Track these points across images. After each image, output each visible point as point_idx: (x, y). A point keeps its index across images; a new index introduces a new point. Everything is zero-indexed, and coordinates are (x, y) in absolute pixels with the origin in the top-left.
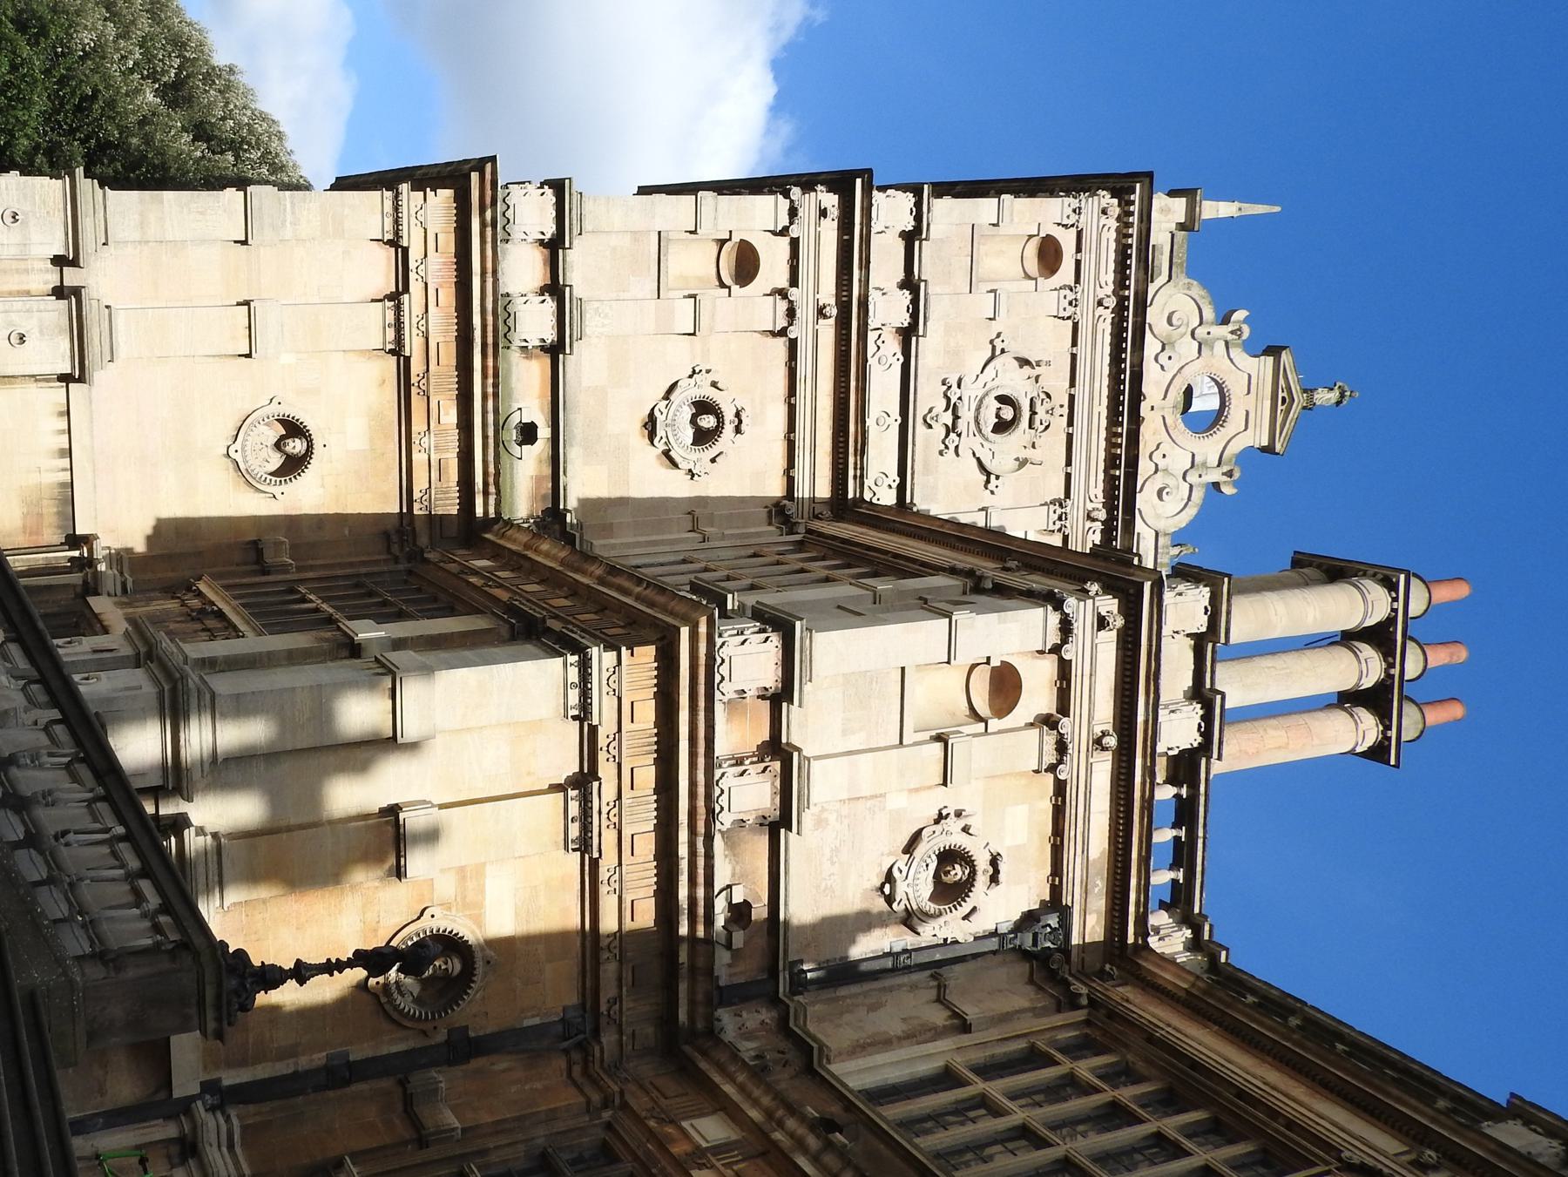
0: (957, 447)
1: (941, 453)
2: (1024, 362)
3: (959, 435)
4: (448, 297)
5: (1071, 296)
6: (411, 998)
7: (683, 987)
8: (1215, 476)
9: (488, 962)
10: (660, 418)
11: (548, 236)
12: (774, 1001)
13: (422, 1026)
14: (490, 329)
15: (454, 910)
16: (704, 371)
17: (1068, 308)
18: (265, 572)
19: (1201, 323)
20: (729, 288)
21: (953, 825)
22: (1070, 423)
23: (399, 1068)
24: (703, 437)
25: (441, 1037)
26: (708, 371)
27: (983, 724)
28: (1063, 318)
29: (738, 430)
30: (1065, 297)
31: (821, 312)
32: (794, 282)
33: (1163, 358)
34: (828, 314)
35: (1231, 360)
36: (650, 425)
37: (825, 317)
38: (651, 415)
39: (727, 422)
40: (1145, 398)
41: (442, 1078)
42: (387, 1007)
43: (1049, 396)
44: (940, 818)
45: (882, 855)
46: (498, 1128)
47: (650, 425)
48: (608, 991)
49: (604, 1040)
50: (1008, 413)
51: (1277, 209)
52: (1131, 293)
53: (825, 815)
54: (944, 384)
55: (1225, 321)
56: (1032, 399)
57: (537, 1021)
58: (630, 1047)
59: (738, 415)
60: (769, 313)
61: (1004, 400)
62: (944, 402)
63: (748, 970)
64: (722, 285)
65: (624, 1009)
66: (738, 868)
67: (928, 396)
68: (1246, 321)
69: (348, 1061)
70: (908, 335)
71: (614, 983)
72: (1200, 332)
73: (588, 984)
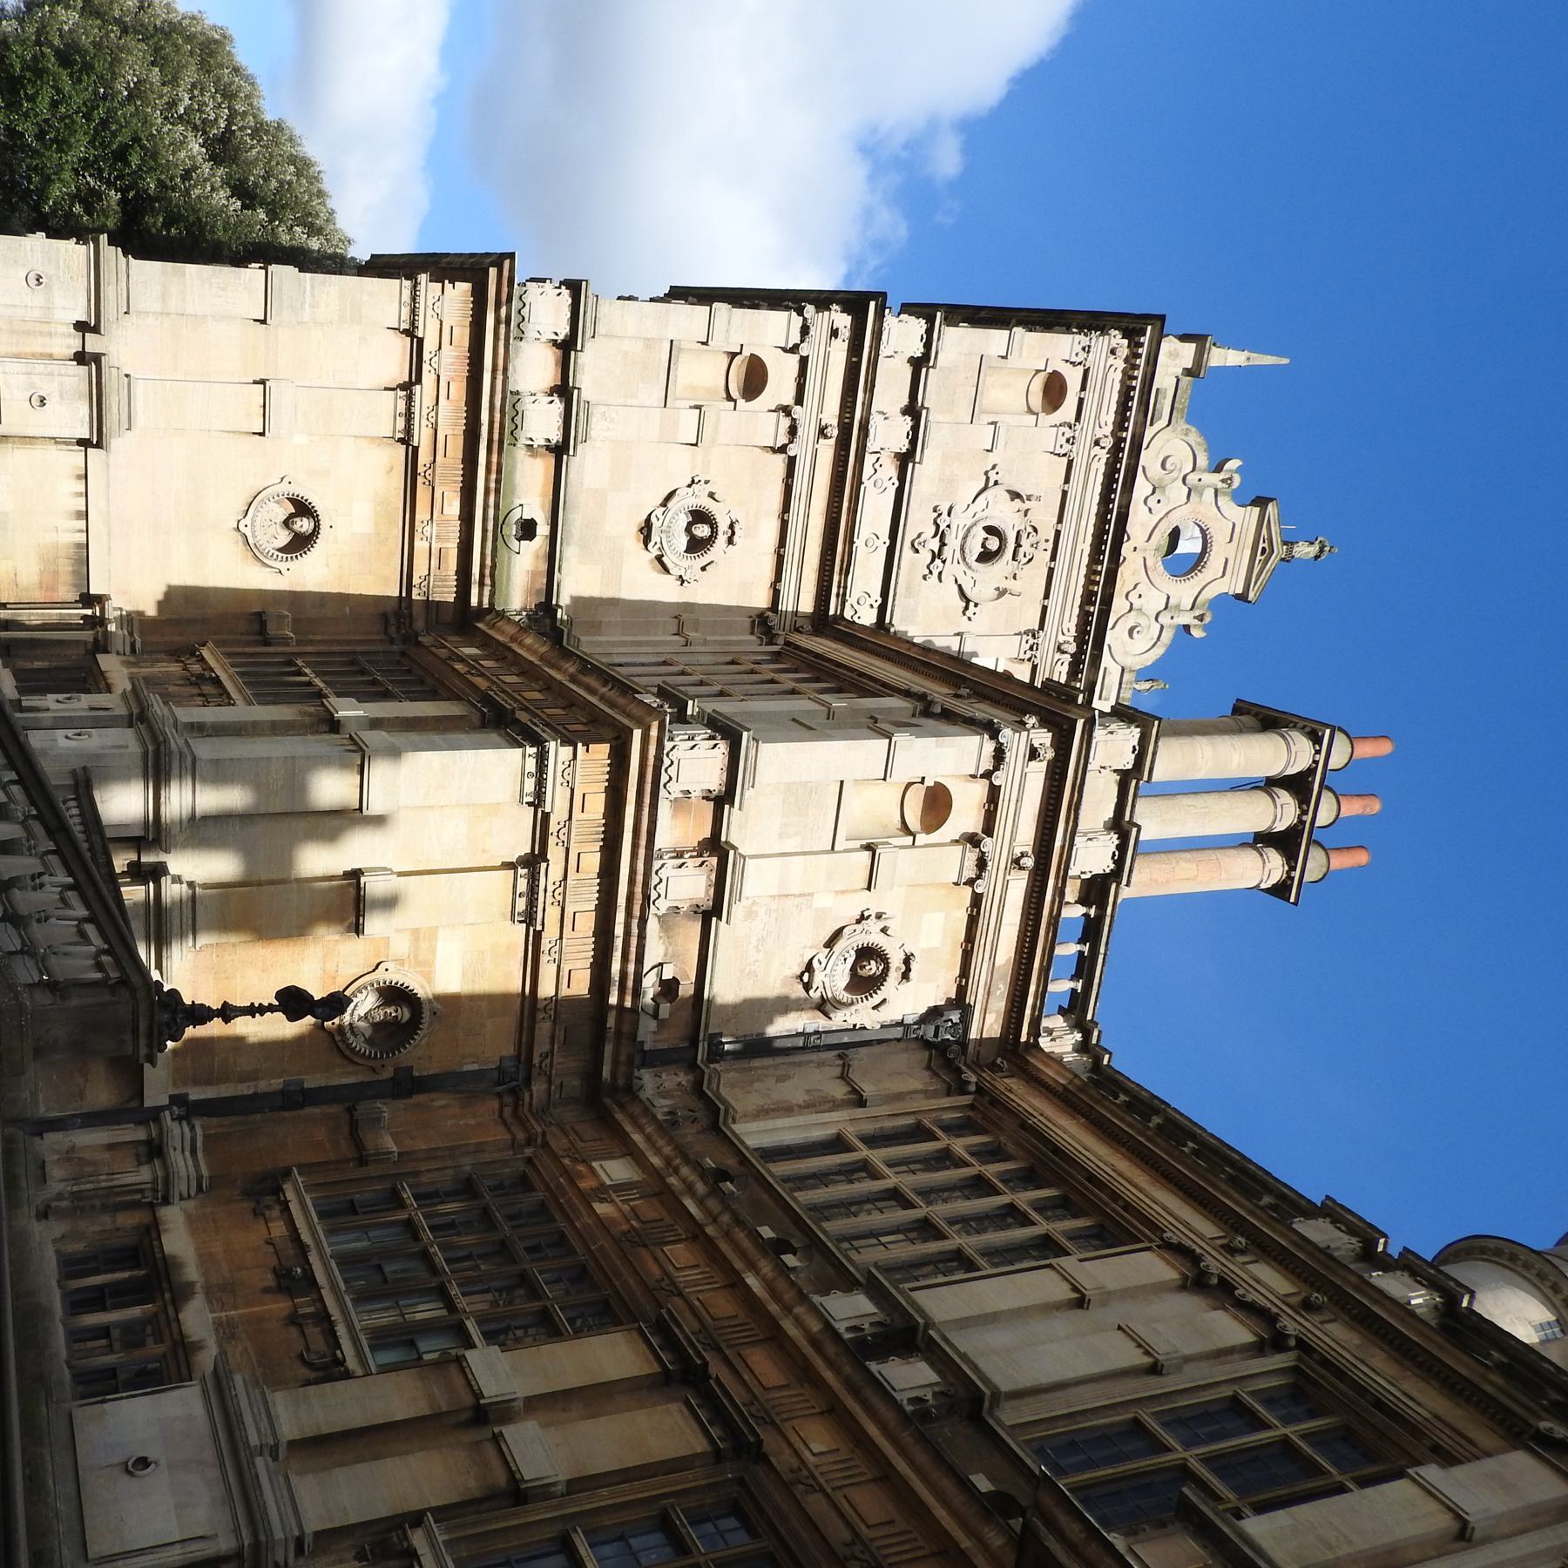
0: (940, 573)
1: (924, 577)
2: (1015, 495)
3: (944, 562)
5: (1069, 433)
6: (363, 1039)
7: (608, 1049)
8: (1187, 619)
10: (656, 524)
12: (692, 1066)
13: (371, 1063)
14: (497, 425)
16: (702, 482)
17: (1065, 445)
18: (267, 643)
19: (1193, 470)
20: (735, 401)
21: (873, 926)
22: (1053, 558)
23: (349, 1097)
24: (696, 546)
25: (388, 1074)
26: (707, 482)
27: (912, 838)
28: (1059, 455)
29: (730, 541)
30: (1063, 434)
31: (822, 432)
32: (799, 400)
33: (1152, 502)
34: (829, 435)
35: (1218, 508)
36: (646, 530)
37: (826, 437)
38: (648, 522)
39: (720, 533)
40: (1129, 539)
41: (386, 1110)
42: (340, 1044)
43: (1035, 530)
44: (862, 918)
45: (805, 947)
46: (431, 1154)
47: (646, 530)
48: (542, 1046)
49: (534, 1088)
50: (993, 544)
51: (1285, 361)
52: (1128, 435)
53: (754, 909)
54: (935, 511)
55: (1218, 469)
56: (1018, 532)
57: (475, 1067)
58: (557, 1096)
59: (731, 526)
60: (771, 429)
61: (991, 530)
62: (933, 529)
63: (672, 1038)
64: (729, 398)
65: (554, 1063)
66: (670, 949)
67: (918, 521)
68: (1239, 470)
69: (303, 1088)
70: (905, 460)
71: (548, 1040)
72: (1192, 478)
73: (524, 1040)
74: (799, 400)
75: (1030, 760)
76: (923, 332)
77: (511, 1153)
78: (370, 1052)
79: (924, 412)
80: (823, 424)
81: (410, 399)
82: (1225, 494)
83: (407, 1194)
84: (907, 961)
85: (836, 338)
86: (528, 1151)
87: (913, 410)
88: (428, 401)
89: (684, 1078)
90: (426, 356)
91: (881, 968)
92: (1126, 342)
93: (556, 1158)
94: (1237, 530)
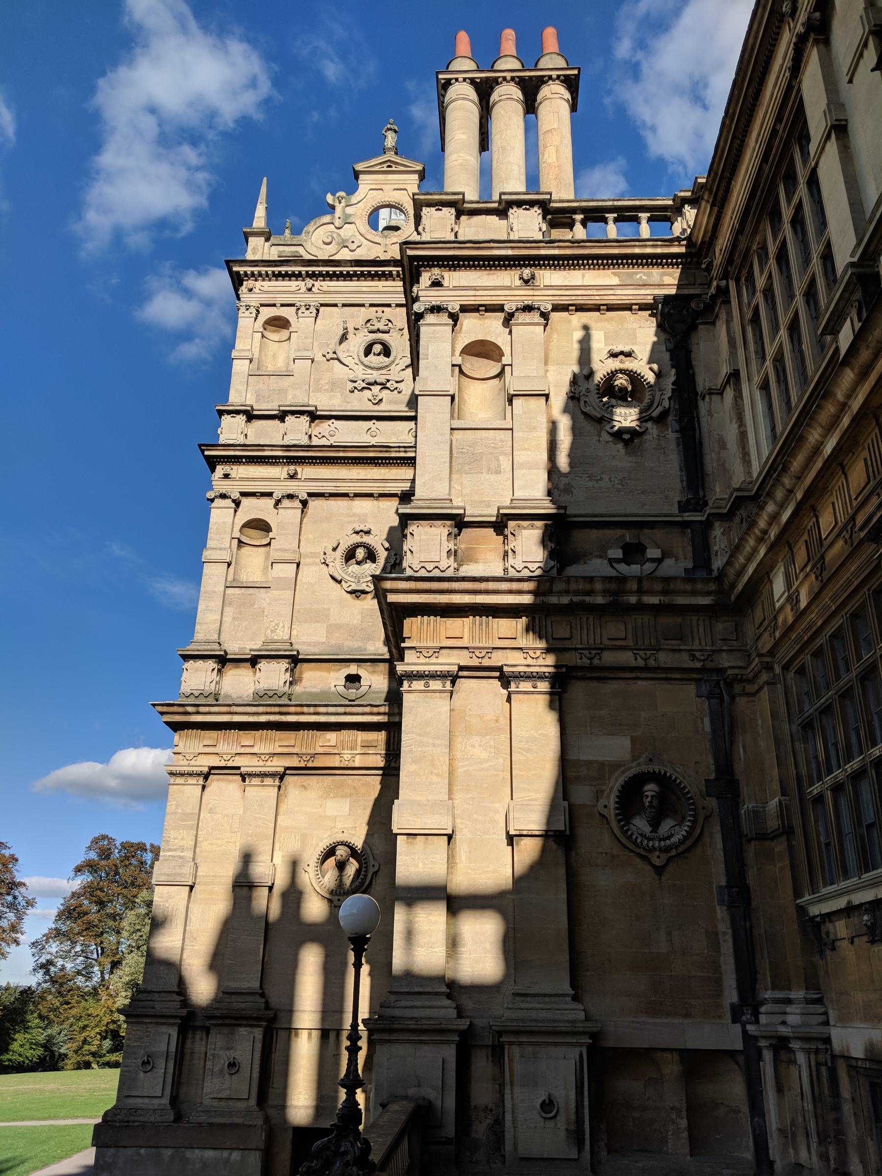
0: (397, 382)
1: (399, 392)
2: (344, 338)
3: (388, 381)
4: (247, 738)
5: (303, 309)
6: (677, 828)
9: (651, 760)
10: (354, 587)
11: (215, 665)
13: (701, 820)
14: (269, 709)
15: (603, 788)
16: (325, 556)
17: (310, 310)
19: (333, 223)
20: (271, 539)
22: (389, 305)
26: (325, 554)
27: (506, 367)
28: (317, 316)
29: (368, 532)
30: (303, 313)
33: (353, 246)
34: (293, 472)
35: (359, 202)
37: (296, 473)
38: (351, 593)
39: (361, 540)
40: (378, 257)
41: (748, 806)
42: (680, 850)
43: (369, 321)
45: (599, 441)
48: (684, 660)
49: (726, 665)
50: (377, 348)
51: (265, 179)
52: (303, 269)
53: (561, 486)
54: (353, 391)
55: (333, 207)
56: (370, 332)
57: (707, 721)
58: (735, 643)
59: (357, 533)
60: (290, 512)
61: (368, 351)
62: (366, 392)
63: (682, 545)
64: (269, 544)
65: (700, 648)
66: (596, 553)
67: (361, 403)
68: (333, 194)
69: (726, 887)
71: (677, 655)
72: (338, 223)
73: (678, 676)
74: (270, 495)
75: (442, 285)
76: (229, 416)
77: (779, 686)
78: (689, 821)
79: (282, 408)
80: (287, 477)
81: (250, 775)
82: (350, 200)
83: (816, 789)
84: (614, 355)
85: (229, 475)
86: (777, 669)
87: (281, 416)
88: (254, 761)
89: (717, 531)
90: (223, 764)
91: (620, 375)
92: (245, 283)
93: (777, 644)
94: (374, 187)
